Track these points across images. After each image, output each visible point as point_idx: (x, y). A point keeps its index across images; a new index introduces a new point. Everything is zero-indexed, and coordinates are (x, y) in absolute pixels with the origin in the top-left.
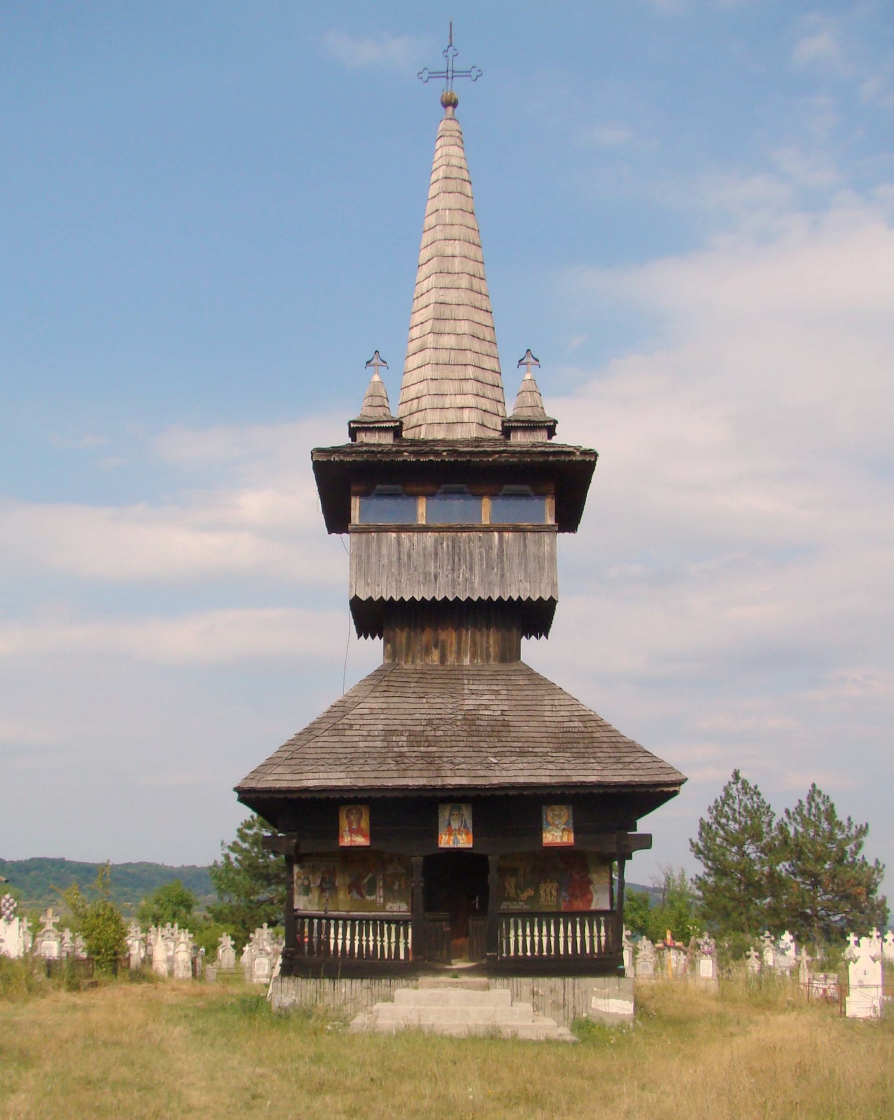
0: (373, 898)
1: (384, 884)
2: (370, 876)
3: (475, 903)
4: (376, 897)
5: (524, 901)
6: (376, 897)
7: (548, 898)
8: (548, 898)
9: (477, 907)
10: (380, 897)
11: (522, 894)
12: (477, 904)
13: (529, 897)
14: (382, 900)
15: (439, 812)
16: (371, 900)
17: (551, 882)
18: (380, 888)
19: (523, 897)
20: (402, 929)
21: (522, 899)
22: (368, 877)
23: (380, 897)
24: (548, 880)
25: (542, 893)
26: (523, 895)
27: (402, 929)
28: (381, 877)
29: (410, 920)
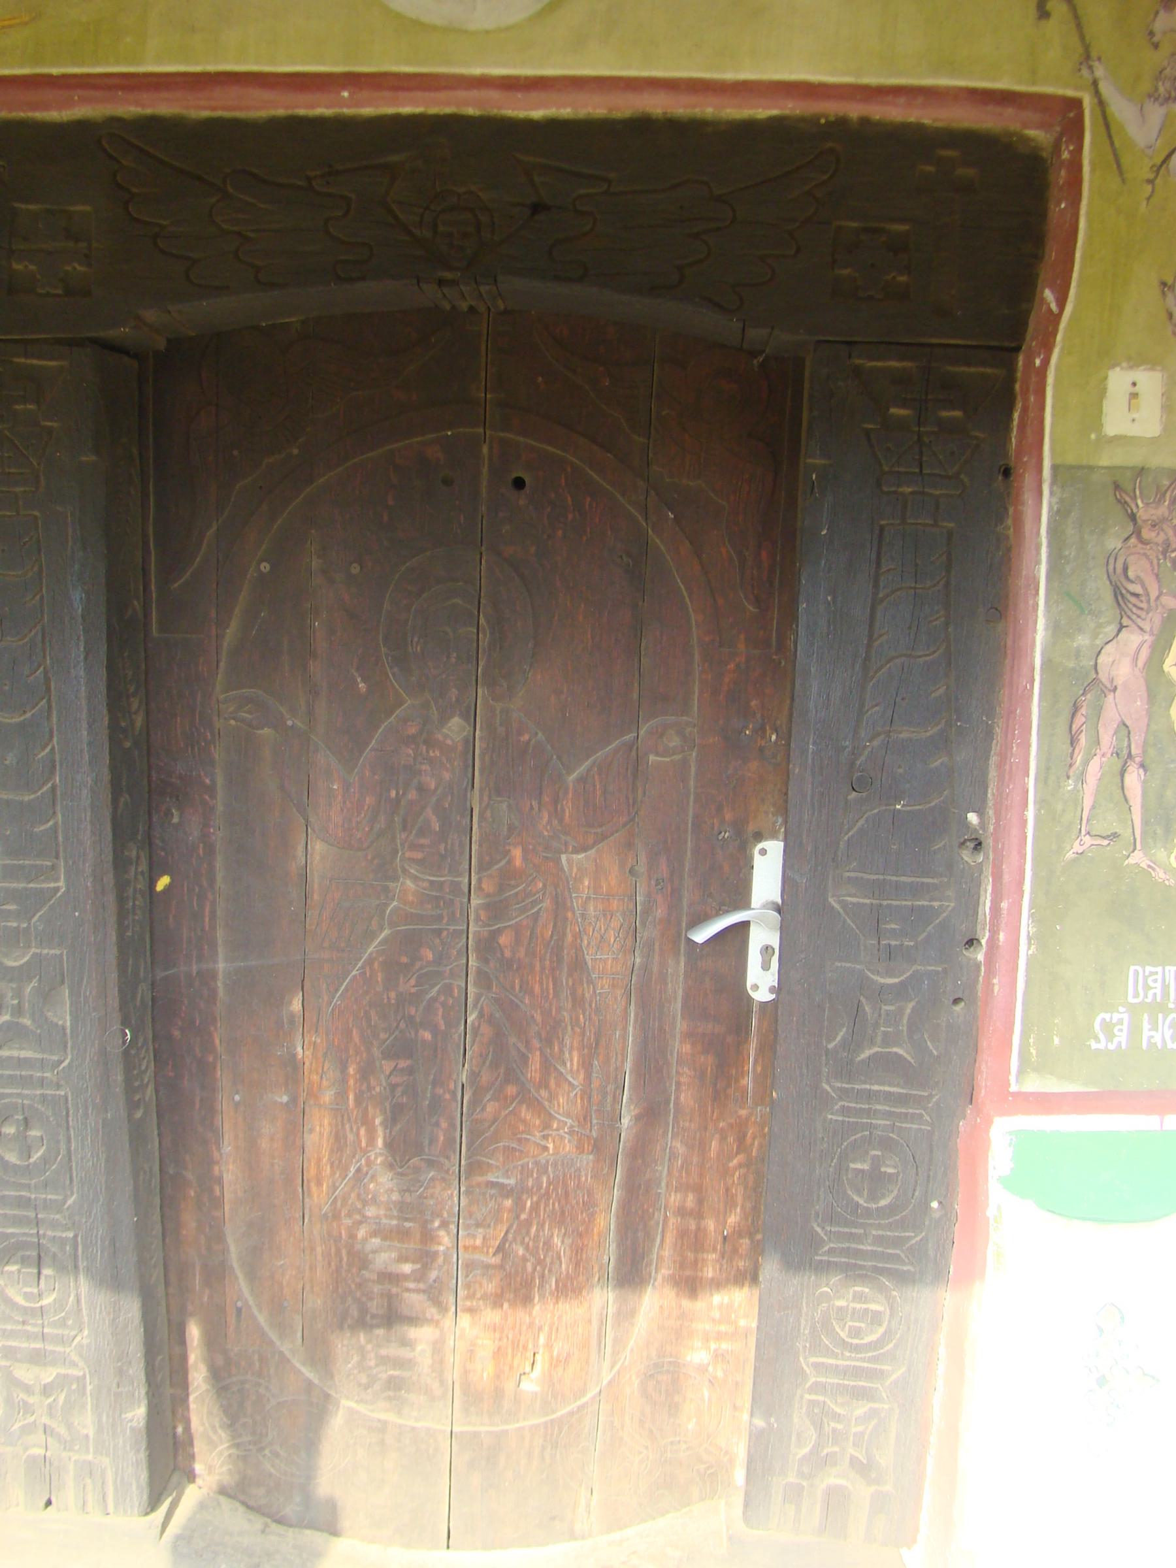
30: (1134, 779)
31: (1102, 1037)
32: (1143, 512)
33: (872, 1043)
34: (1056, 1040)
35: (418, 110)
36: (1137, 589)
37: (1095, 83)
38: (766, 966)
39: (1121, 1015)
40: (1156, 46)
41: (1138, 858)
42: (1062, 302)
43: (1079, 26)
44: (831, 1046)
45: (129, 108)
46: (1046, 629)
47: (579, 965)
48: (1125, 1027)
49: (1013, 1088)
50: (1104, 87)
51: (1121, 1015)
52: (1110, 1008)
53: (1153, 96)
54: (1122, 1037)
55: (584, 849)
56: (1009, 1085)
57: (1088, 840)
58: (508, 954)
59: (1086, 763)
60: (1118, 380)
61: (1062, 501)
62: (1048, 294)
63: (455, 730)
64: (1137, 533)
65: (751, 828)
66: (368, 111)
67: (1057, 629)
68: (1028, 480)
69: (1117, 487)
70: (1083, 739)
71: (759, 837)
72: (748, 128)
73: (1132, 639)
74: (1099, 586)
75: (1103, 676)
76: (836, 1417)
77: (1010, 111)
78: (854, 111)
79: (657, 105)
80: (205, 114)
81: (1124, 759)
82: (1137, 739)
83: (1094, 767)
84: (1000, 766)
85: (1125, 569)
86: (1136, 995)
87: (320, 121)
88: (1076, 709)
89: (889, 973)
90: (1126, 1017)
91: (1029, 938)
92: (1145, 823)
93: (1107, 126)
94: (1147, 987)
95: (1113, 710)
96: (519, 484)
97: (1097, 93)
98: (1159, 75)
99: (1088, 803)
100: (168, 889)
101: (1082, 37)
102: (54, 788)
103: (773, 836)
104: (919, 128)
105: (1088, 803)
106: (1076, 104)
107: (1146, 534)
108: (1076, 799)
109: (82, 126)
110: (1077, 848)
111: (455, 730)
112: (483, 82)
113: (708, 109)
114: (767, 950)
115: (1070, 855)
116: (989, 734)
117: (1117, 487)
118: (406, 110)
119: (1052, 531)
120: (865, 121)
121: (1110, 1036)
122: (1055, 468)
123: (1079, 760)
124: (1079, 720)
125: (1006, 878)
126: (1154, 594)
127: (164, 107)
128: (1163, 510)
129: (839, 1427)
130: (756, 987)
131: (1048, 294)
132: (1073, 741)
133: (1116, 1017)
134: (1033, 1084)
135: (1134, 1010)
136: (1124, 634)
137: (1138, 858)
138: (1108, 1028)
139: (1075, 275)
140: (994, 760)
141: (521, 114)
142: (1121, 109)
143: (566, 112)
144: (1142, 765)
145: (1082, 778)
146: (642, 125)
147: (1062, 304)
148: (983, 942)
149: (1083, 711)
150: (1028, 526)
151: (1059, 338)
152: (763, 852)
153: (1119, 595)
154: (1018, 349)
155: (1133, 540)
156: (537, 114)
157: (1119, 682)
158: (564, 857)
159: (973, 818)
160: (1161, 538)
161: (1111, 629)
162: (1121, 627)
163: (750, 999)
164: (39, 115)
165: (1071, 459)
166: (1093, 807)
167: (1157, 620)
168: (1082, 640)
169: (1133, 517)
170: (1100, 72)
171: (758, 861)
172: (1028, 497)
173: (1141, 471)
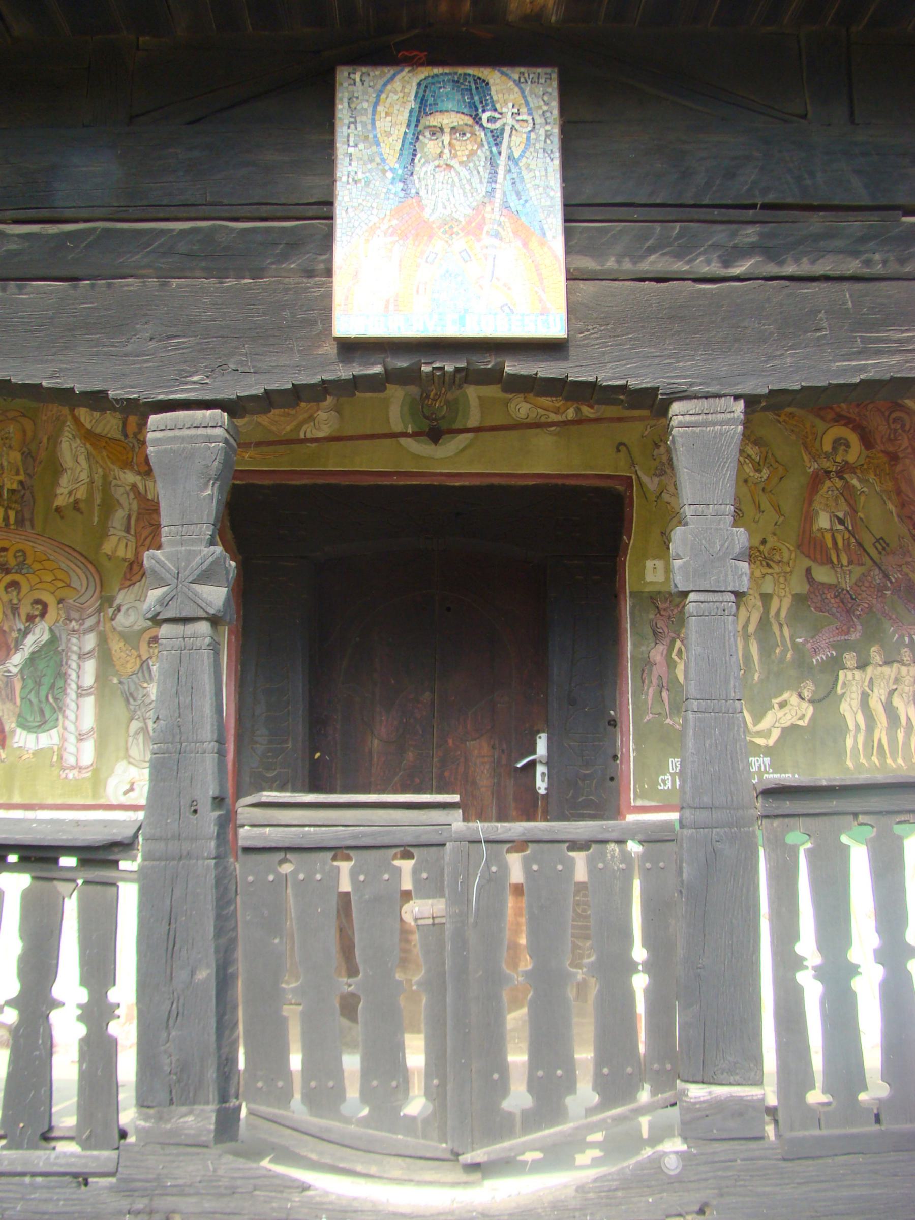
0: (47, 739)
1: (101, 677)
2: (39, 635)
3: (533, 764)
4: (63, 739)
5: (768, 751)
6: (63, 739)
7: (881, 733)
8: (881, 733)
9: (541, 786)
10: (81, 738)
11: (758, 719)
12: (541, 769)
13: (790, 732)
14: (88, 753)
15: (342, 110)
16: (36, 753)
17: (887, 663)
18: (82, 693)
19: (767, 734)
20: (71, 908)
21: (761, 741)
22: (30, 643)
23: (81, 738)
24: (876, 655)
25: (849, 709)
26: (764, 725)
27: (71, 908)
28: (90, 642)
29: (125, 846)
30: (665, 694)
31: (662, 785)
32: (660, 604)
33: (582, 795)
34: (646, 786)
35: (418, 483)
36: (661, 631)
37: (636, 471)
38: (543, 781)
39: (668, 776)
40: (655, 459)
41: (668, 721)
42: (629, 540)
43: (630, 454)
44: (568, 797)
45: (321, 481)
46: (631, 645)
47: (474, 783)
48: (670, 781)
49: (633, 804)
50: (639, 472)
51: (668, 776)
52: (664, 774)
53: (655, 475)
54: (669, 785)
55: (475, 739)
56: (630, 803)
57: (651, 716)
58: (447, 779)
59: (648, 689)
60: (649, 564)
61: (633, 603)
62: (625, 537)
63: (427, 696)
64: (659, 612)
65: (535, 729)
66: (402, 483)
67: (634, 645)
68: (622, 596)
69: (651, 598)
70: (646, 681)
71: (538, 732)
72: (526, 488)
73: (660, 647)
74: (648, 631)
75: (651, 660)
76: (580, 947)
77: (609, 481)
78: (560, 482)
79: (496, 481)
80: (347, 483)
81: (661, 688)
82: (665, 681)
83: (651, 691)
84: (620, 694)
85: (656, 624)
86: (673, 769)
87: (386, 486)
88: (643, 671)
89: (587, 770)
90: (670, 778)
91: (633, 750)
92: (670, 708)
93: (641, 484)
94: (676, 766)
95: (656, 671)
96: (449, 609)
97: (637, 474)
98: (656, 469)
99: (650, 702)
100: (319, 757)
101: (631, 457)
102: (288, 711)
103: (544, 732)
104: (581, 487)
105: (650, 702)
106: (630, 478)
107: (662, 613)
108: (646, 702)
109: (305, 486)
110: (647, 718)
111: (427, 696)
112: (441, 474)
113: (513, 482)
114: (543, 774)
115: (645, 720)
116: (615, 683)
117: (651, 598)
118: (414, 483)
119: (631, 613)
120: (564, 485)
121: (665, 784)
122: (630, 592)
123: (646, 688)
124: (645, 675)
125: (624, 730)
126: (666, 632)
127: (333, 481)
128: (667, 605)
129: (581, 951)
130: (540, 788)
131: (625, 537)
132: (643, 682)
133: (666, 777)
134: (639, 803)
135: (671, 774)
136: (657, 646)
137: (668, 721)
138: (664, 781)
139: (633, 531)
140: (617, 692)
141: (452, 484)
142: (645, 479)
143: (467, 484)
144: (668, 690)
145: (647, 694)
146: (491, 487)
147: (629, 540)
148: (619, 756)
149: (646, 672)
150: (623, 612)
151: (629, 551)
152: (540, 737)
153: (655, 633)
154: (617, 556)
155: (658, 615)
156: (457, 484)
157: (657, 662)
158: (468, 743)
159: (612, 712)
160: (667, 614)
161: (653, 644)
162: (656, 643)
163: (538, 793)
164: (290, 483)
165: (635, 589)
166: (652, 704)
167: (668, 641)
168: (643, 648)
169: (657, 608)
170: (637, 468)
171: (538, 741)
172: (622, 603)
173: (659, 592)
